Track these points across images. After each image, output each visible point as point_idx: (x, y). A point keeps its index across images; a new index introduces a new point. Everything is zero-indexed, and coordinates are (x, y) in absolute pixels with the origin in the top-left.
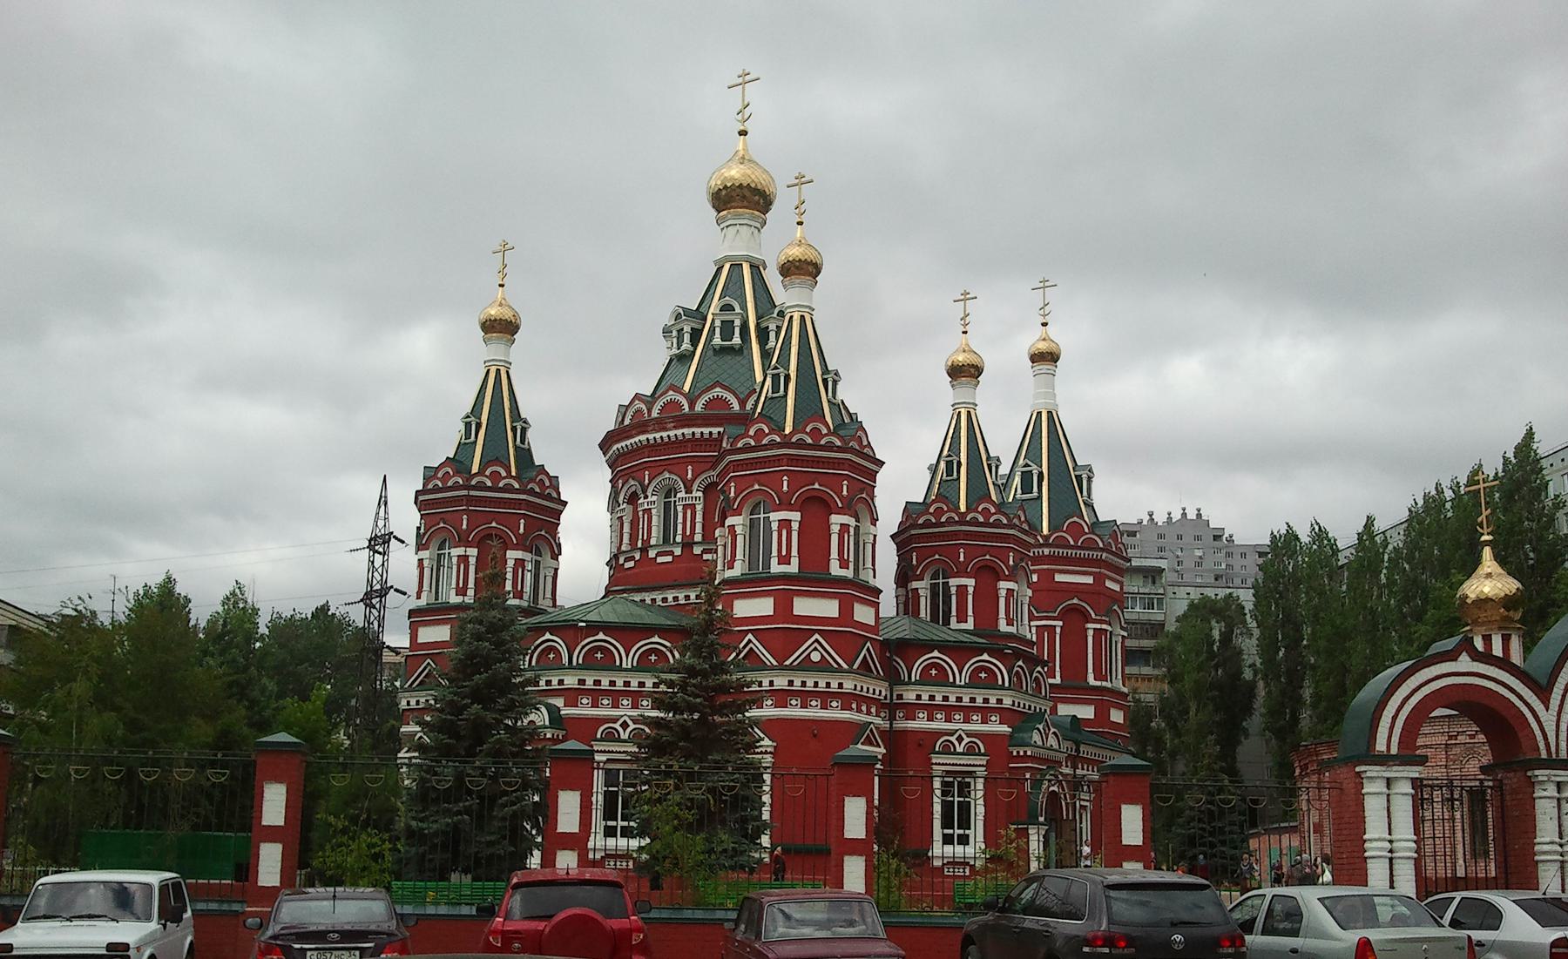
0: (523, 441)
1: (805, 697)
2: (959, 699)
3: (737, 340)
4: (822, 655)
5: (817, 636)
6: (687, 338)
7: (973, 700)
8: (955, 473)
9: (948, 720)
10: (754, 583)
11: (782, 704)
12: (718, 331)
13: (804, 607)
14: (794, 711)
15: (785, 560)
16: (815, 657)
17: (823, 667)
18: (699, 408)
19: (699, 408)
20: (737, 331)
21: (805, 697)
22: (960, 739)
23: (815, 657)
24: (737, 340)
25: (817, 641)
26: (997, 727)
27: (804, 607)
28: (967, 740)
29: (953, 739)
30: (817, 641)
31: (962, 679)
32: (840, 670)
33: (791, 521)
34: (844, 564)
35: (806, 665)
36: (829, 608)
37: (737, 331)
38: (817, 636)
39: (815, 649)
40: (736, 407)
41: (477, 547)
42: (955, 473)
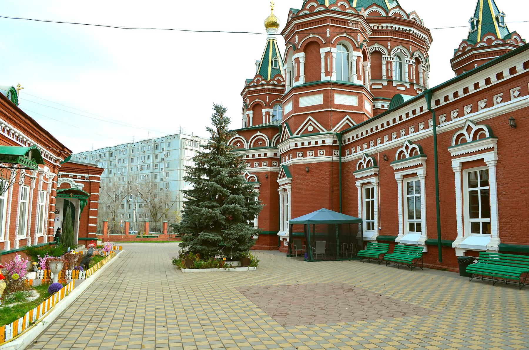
0: (276, 66)
1: (304, 150)
4: (314, 127)
5: (310, 117)
8: (476, 27)
11: (294, 157)
13: (305, 102)
14: (300, 159)
15: (297, 79)
16: (310, 129)
17: (315, 132)
21: (304, 150)
23: (310, 129)
25: (310, 120)
27: (305, 102)
30: (310, 120)
33: (298, 58)
34: (359, 79)
35: (306, 134)
36: (317, 100)
38: (310, 117)
39: (311, 125)
41: (253, 110)
42: (476, 27)
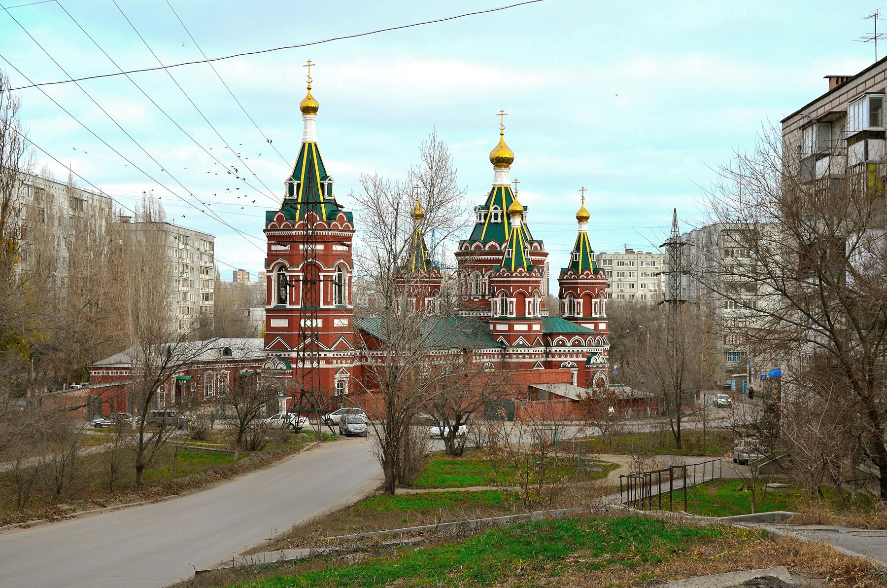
2: (569, 351)
3: (499, 220)
6: (483, 217)
7: (573, 351)
9: (566, 357)
10: (503, 319)
12: (493, 217)
18: (487, 248)
19: (487, 248)
20: (499, 217)
22: (569, 363)
24: (499, 220)
26: (581, 359)
28: (571, 363)
29: (567, 363)
31: (570, 344)
32: (528, 347)
37: (499, 217)
40: (498, 248)
